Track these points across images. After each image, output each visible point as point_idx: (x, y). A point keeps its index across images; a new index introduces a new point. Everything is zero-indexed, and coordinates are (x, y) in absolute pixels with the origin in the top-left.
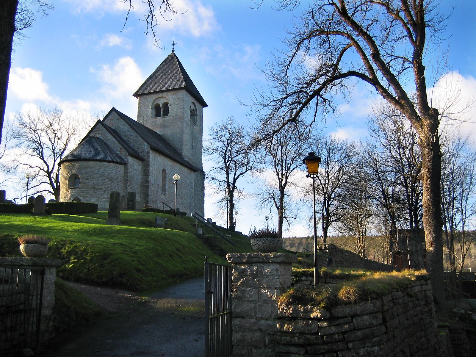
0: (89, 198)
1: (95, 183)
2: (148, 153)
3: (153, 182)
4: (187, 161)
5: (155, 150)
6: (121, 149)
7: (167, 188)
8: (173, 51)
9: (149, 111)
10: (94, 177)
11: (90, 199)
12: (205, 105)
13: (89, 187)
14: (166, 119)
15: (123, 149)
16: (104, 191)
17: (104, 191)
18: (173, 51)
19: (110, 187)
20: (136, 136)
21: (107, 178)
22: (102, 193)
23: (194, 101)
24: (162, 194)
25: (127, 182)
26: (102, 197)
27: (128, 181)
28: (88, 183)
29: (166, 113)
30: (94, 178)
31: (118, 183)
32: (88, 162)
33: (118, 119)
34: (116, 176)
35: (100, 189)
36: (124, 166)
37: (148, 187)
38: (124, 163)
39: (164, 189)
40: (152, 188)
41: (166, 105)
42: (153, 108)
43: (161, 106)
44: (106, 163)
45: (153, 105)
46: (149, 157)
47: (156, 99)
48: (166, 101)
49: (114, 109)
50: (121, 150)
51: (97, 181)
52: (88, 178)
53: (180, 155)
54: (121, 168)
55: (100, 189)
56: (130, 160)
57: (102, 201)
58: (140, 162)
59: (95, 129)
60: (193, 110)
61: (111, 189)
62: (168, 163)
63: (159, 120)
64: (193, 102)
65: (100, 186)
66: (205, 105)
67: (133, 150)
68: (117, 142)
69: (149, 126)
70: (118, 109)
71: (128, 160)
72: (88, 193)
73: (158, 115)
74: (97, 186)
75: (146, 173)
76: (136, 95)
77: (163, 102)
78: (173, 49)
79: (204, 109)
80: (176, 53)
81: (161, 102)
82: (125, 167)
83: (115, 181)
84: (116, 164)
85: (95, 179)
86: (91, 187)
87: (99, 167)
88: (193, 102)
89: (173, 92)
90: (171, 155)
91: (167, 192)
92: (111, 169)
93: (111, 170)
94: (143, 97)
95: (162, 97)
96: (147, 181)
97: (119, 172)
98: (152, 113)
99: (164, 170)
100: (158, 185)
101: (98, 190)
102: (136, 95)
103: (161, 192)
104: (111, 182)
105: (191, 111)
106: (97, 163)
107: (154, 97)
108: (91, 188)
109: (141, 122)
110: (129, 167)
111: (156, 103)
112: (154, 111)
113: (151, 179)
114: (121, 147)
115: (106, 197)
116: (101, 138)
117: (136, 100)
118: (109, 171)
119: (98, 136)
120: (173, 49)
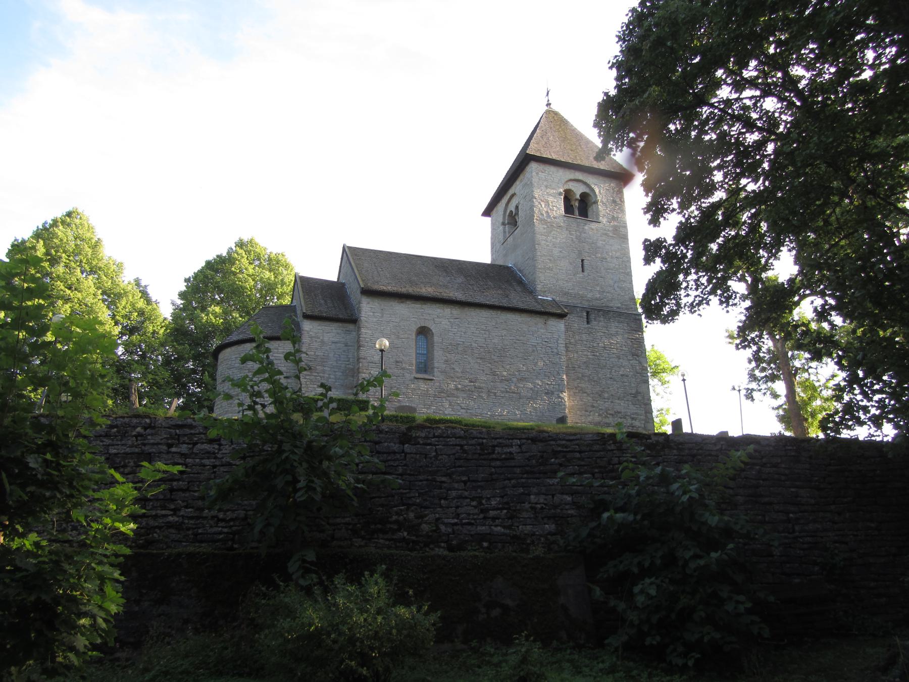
2: (360, 303)
5: (369, 293)
8: (548, 105)
18: (548, 105)
23: (579, 175)
39: (425, 367)
41: (517, 207)
42: (506, 222)
53: (527, 289)
56: (308, 326)
58: (351, 327)
60: (584, 197)
72: (221, 407)
76: (487, 212)
78: (548, 101)
80: (554, 107)
81: (512, 207)
88: (571, 180)
98: (505, 232)
99: (423, 332)
100: (397, 362)
106: (234, 348)
111: (508, 211)
117: (488, 220)
120: (548, 101)
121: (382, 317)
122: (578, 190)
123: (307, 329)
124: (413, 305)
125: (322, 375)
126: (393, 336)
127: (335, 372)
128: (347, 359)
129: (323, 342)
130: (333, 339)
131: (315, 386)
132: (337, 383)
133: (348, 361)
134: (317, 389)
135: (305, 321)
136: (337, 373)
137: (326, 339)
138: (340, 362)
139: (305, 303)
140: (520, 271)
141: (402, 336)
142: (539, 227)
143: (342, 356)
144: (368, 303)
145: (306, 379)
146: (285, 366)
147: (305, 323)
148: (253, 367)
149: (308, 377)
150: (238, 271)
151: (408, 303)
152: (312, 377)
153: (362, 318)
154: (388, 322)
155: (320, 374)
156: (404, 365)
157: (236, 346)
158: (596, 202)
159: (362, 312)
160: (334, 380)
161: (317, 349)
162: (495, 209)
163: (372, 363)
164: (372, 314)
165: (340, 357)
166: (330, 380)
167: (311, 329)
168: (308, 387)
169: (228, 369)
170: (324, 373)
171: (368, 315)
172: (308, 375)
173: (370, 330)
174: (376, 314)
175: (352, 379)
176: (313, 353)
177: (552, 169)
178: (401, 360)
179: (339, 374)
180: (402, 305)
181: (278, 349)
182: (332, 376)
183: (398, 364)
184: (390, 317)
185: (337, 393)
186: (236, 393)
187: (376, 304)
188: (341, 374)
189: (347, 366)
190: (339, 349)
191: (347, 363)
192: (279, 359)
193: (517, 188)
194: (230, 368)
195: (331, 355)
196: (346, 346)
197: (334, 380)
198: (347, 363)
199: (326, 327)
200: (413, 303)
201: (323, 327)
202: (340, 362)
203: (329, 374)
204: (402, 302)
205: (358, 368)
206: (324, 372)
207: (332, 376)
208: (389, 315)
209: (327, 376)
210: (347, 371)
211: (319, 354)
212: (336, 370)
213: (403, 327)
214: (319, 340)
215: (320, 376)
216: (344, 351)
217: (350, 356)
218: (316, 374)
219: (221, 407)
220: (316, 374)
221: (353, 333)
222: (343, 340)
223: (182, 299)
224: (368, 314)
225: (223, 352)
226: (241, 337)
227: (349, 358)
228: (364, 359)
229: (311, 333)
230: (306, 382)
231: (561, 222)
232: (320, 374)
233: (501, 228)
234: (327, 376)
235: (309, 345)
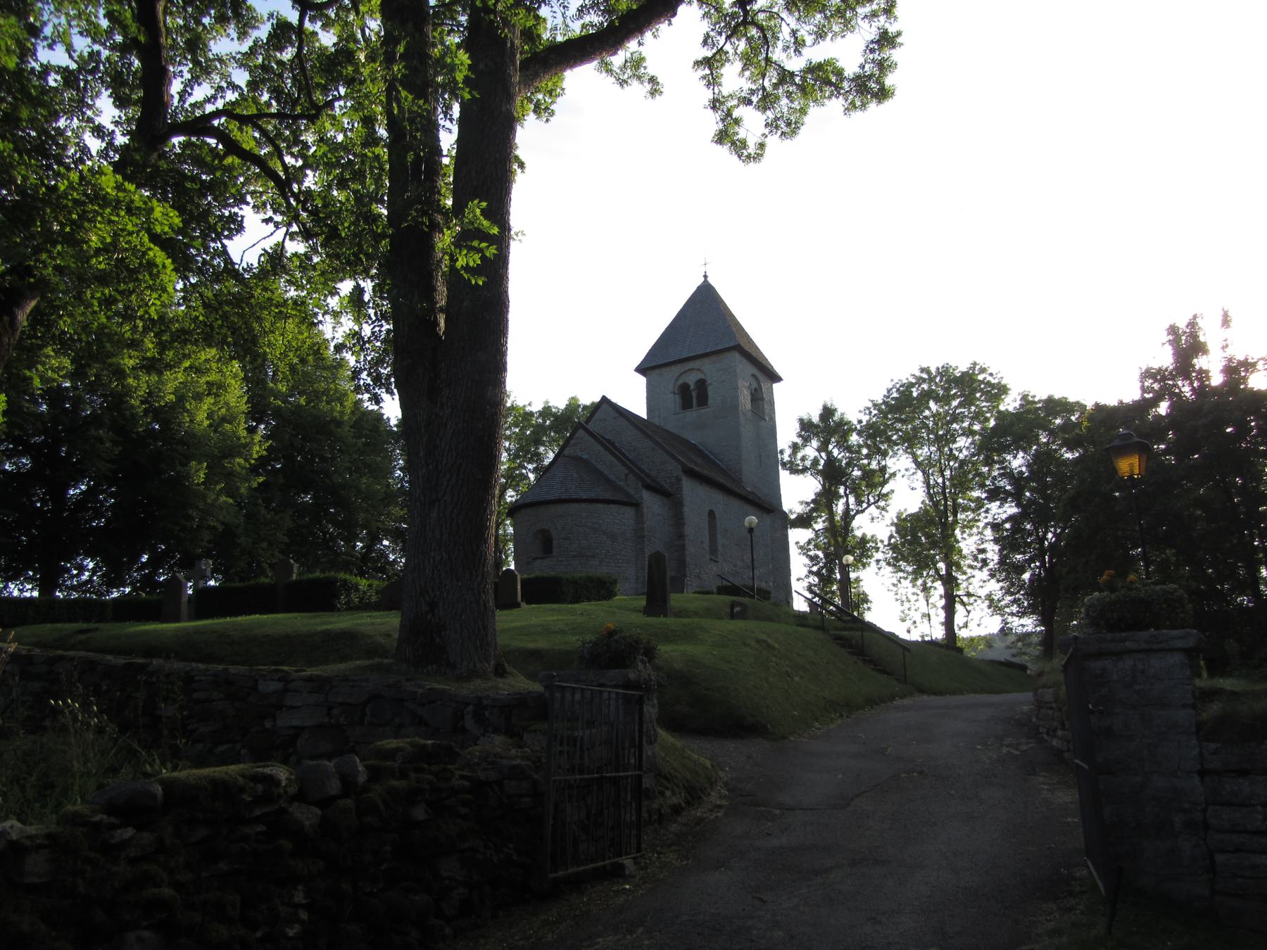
2: (679, 480)
4: (753, 493)
5: (691, 474)
6: (626, 475)
7: (720, 548)
8: (705, 276)
9: (671, 400)
12: (777, 379)
13: (571, 553)
14: (703, 411)
15: (631, 475)
18: (705, 276)
20: (653, 449)
21: (604, 534)
24: (711, 559)
29: (703, 400)
32: (567, 505)
33: (615, 418)
37: (683, 548)
38: (636, 505)
40: (690, 550)
41: (702, 384)
42: (676, 391)
43: (692, 387)
44: (600, 506)
45: (677, 387)
47: (681, 374)
48: (700, 376)
50: (626, 478)
54: (629, 512)
59: (572, 442)
60: (755, 389)
62: (717, 500)
63: (691, 415)
64: (753, 375)
66: (777, 379)
67: (648, 476)
68: (617, 462)
69: (670, 427)
70: (614, 399)
71: (641, 496)
73: (686, 404)
75: (678, 519)
76: (642, 369)
77: (695, 380)
79: (776, 386)
81: (691, 379)
89: (713, 358)
90: (721, 479)
91: (720, 556)
94: (655, 373)
95: (693, 369)
96: (681, 536)
98: (675, 402)
102: (642, 369)
103: (708, 557)
105: (751, 394)
106: (583, 505)
107: (677, 370)
109: (656, 421)
110: (645, 510)
111: (680, 382)
112: (678, 398)
113: (689, 530)
114: (627, 472)
116: (585, 457)
117: (642, 381)
119: (579, 454)
122: (755, 385)
140: (711, 453)
142: (742, 418)
158: (762, 399)
162: (657, 371)
177: (745, 361)
193: (708, 369)
205: (684, 545)
231: (749, 414)
233: (671, 396)
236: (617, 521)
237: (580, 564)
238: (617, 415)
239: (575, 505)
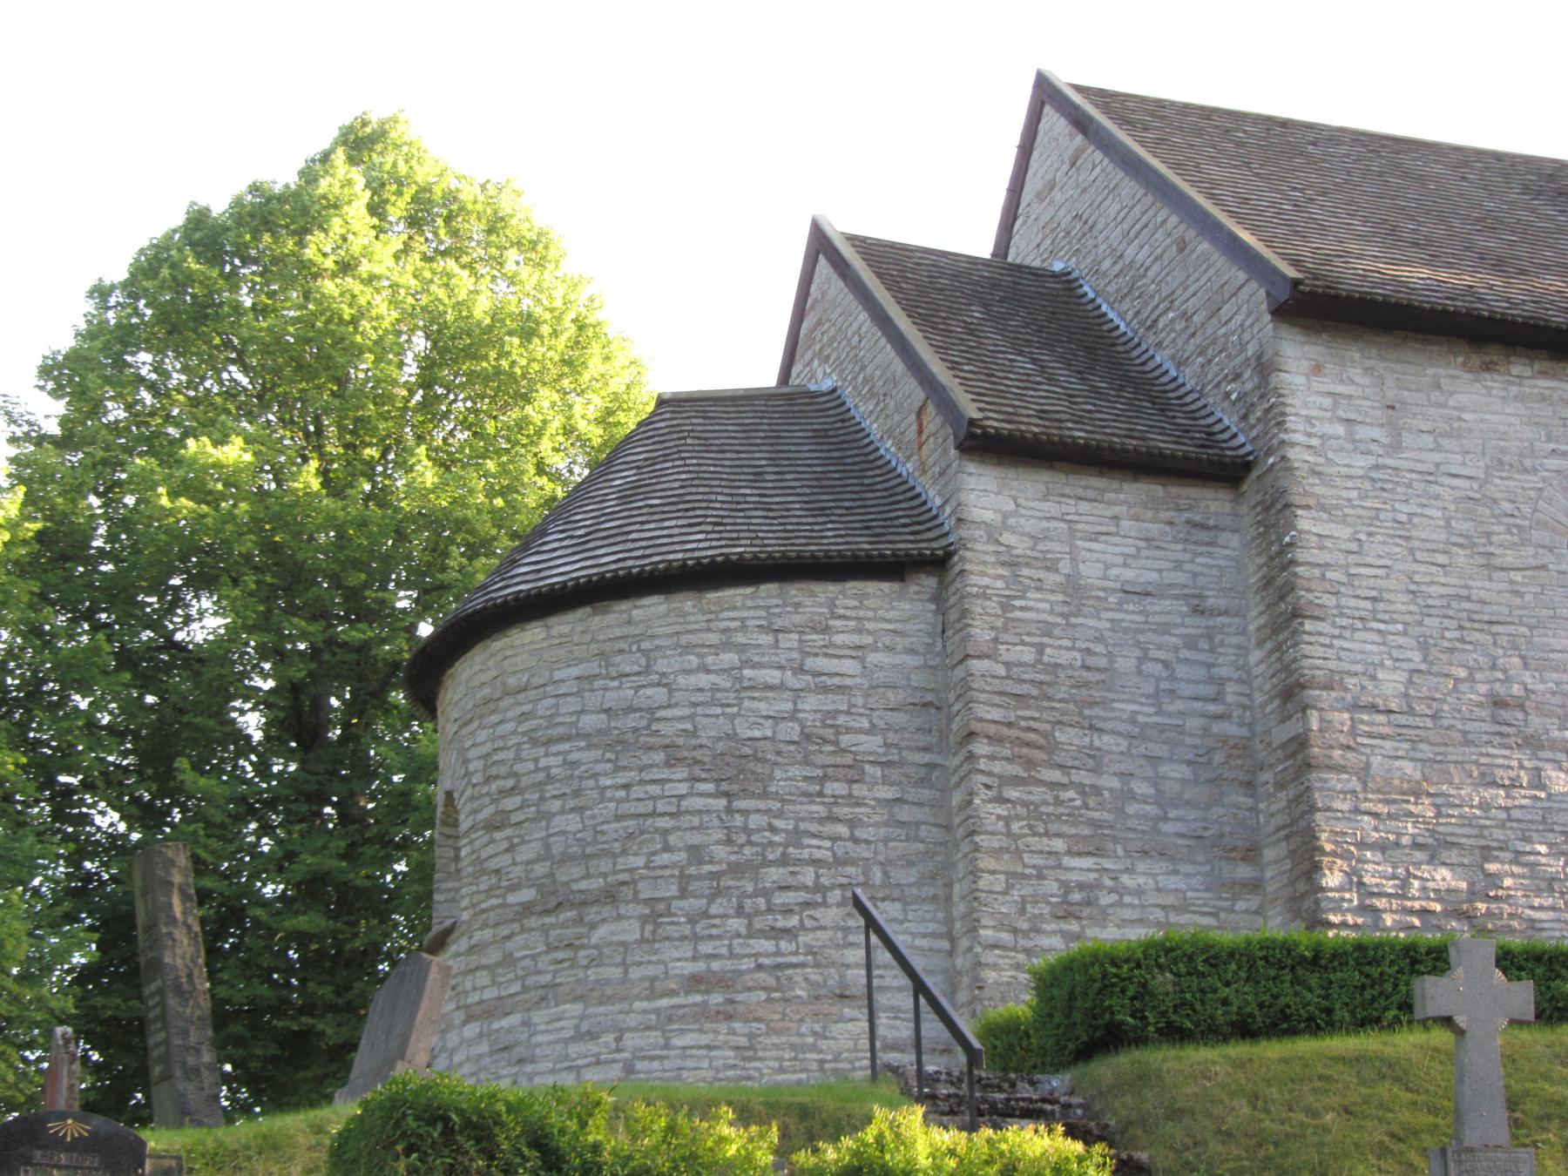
0: (514, 1020)
1: (557, 847)
2: (1265, 367)
3: (1391, 683)
10: (550, 779)
11: (526, 1023)
16: (656, 914)
17: (656, 914)
19: (720, 851)
20: (1182, 246)
22: (630, 931)
25: (971, 757)
26: (635, 973)
27: (971, 735)
28: (506, 860)
30: (550, 791)
31: (839, 788)
34: (793, 716)
35: (610, 896)
36: (929, 582)
44: (651, 608)
46: (1275, 417)
49: (1046, 93)
51: (572, 823)
52: (510, 803)
55: (610, 896)
57: (632, 1020)
58: (1212, 502)
61: (736, 869)
65: (605, 865)
72: (508, 960)
74: (576, 871)
82: (938, 598)
83: (789, 777)
84: (794, 591)
85: (556, 805)
86: (527, 895)
87: (593, 667)
92: (726, 646)
93: (729, 658)
97: (850, 666)
100: (1498, 703)
101: (591, 914)
104: (727, 795)
106: (564, 625)
108: (527, 909)
114: (919, 395)
115: (689, 968)
118: (704, 680)
121: (1395, 447)
123: (988, 516)
124: (1542, 383)
125: (1085, 778)
126: (1461, 557)
127: (1154, 760)
128: (1210, 690)
129: (1074, 588)
130: (1129, 574)
131: (1059, 845)
132: (1168, 827)
133: (1214, 700)
134: (1069, 861)
135: (971, 467)
136: (1164, 769)
137: (1090, 572)
138: (1180, 705)
139: (954, 366)
141: (1510, 558)
143: (1181, 671)
144: (1317, 369)
145: (1001, 800)
146: (872, 730)
147: (971, 482)
148: (694, 734)
149: (1013, 793)
150: (329, 264)
151: (1515, 370)
152: (1038, 794)
153: (1292, 454)
154: (1431, 476)
155: (1076, 776)
156: (1535, 721)
157: (580, 613)
159: (1292, 422)
160: (1151, 809)
161: (1047, 629)
163: (1373, 708)
164: (1340, 430)
165: (1172, 677)
166: (1131, 809)
167: (1006, 516)
168: (1018, 853)
169: (535, 742)
170: (1096, 771)
171: (1323, 437)
172: (1016, 781)
173: (1344, 520)
174: (1363, 432)
175: (1245, 801)
176: (1028, 655)
178: (1516, 690)
179: (1175, 772)
180: (1494, 382)
181: (826, 630)
182: (1141, 788)
183: (1505, 714)
184: (1438, 448)
185: (1174, 882)
186: (597, 884)
187: (1356, 373)
188: (1185, 772)
189: (1217, 728)
190: (1164, 629)
191: (1212, 708)
192: (842, 689)
194: (550, 741)
195: (1126, 663)
196: (1198, 611)
197: (1151, 809)
198: (1212, 708)
199: (1084, 507)
200: (1543, 374)
201: (1070, 506)
202: (1180, 705)
203: (1126, 776)
204: (1488, 367)
205: (1300, 743)
206: (1095, 760)
207: (1141, 788)
208: (1428, 440)
209: (1115, 783)
210: (1218, 758)
211: (1065, 657)
212: (1160, 750)
213: (1507, 507)
214: (1051, 579)
215: (1081, 789)
216: (1191, 644)
217: (1223, 672)
218: (1057, 776)
219: (508, 960)
220: (1057, 776)
221: (1223, 537)
222: (1179, 577)
223: (56, 394)
224: (1320, 428)
225: (497, 644)
226: (606, 560)
227: (1222, 682)
228: (1328, 687)
229: (1006, 538)
230: (1007, 820)
232: (1076, 776)
234: (1115, 783)
235: (1006, 608)
236: (773, 676)
237: (551, 948)
238: (1079, 139)
239: (529, 637)
